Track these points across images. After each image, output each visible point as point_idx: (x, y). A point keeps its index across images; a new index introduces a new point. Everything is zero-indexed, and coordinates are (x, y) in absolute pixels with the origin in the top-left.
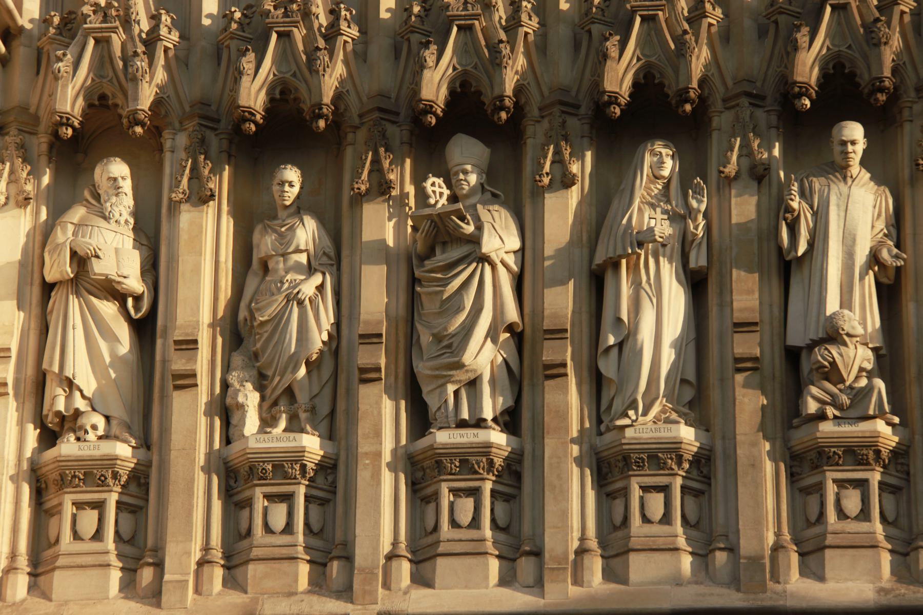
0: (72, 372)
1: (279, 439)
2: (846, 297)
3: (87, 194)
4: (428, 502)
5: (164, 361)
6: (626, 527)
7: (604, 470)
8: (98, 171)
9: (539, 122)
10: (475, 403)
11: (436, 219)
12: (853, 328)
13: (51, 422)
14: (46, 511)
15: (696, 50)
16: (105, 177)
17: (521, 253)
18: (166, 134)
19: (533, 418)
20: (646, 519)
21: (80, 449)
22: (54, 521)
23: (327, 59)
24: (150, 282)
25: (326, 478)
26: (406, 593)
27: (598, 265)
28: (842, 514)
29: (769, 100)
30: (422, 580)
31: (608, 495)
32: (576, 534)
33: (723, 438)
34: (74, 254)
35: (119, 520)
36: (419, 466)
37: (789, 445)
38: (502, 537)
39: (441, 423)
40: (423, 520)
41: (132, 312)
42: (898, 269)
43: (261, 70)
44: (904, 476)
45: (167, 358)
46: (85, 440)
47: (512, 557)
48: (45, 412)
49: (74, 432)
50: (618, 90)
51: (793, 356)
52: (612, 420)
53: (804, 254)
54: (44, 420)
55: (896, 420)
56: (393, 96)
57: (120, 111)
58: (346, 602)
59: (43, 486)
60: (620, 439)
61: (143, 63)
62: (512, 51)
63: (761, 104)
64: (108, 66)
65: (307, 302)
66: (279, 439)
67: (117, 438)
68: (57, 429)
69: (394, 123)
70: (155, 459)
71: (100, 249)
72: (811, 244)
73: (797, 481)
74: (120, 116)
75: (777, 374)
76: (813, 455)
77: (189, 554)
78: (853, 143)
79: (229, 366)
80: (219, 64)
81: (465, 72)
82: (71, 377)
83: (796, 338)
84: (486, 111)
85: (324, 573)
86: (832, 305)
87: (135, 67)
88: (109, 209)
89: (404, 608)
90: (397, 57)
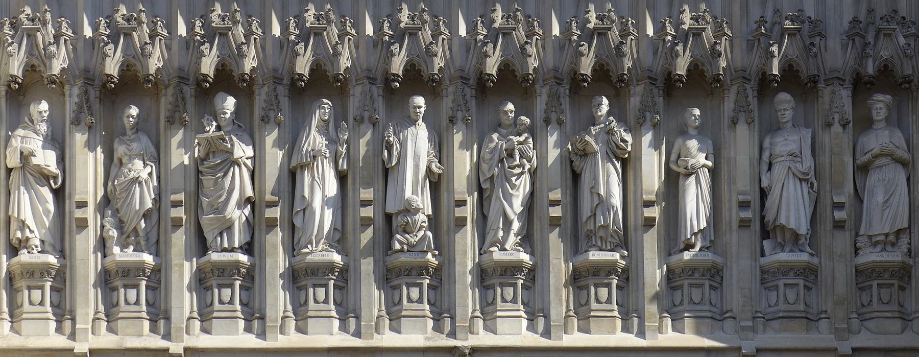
0: (24, 217)
1: (131, 256)
2: (414, 188)
3: (26, 119)
4: (208, 290)
5: (71, 212)
6: (306, 305)
7: (296, 275)
8: (32, 107)
9: (262, 87)
10: (231, 239)
11: (210, 140)
12: (418, 205)
13: (15, 242)
14: (15, 289)
15: (343, 52)
16: (36, 111)
17: (253, 158)
18: (67, 87)
19: (260, 247)
20: (316, 301)
21: (30, 258)
22: (19, 294)
23: (151, 49)
24: (61, 168)
25: (156, 277)
26: (197, 337)
27: (293, 167)
28: (410, 300)
29: (378, 81)
30: (206, 330)
31: (297, 288)
32: (282, 309)
33: (354, 260)
34: (22, 153)
35: (52, 296)
36: (203, 271)
37: (386, 264)
38: (245, 309)
39: (213, 249)
40: (205, 299)
41: (53, 184)
42: (440, 175)
43: (116, 54)
44: (440, 281)
45: (72, 211)
46: (32, 253)
47: (250, 319)
48: (11, 238)
49: (27, 248)
50: (303, 73)
51: (389, 218)
52: (300, 249)
53: (396, 164)
54: (11, 242)
55: (437, 253)
56: (186, 70)
57: (43, 75)
58: (168, 341)
59: (13, 276)
60: (304, 260)
61: (54, 49)
62: (248, 48)
63: (374, 83)
64: (35, 48)
65: (144, 182)
66: (131, 256)
67: (48, 252)
68: (17, 246)
69: (187, 84)
70: (68, 264)
71: (35, 151)
72: (398, 160)
73: (390, 282)
74: (43, 77)
75: (381, 227)
76: (397, 270)
77: (88, 314)
78: (420, 107)
79: (104, 216)
80: (93, 49)
81: (223, 59)
82: (24, 220)
83: (390, 209)
84: (235, 81)
85: (156, 325)
86: (408, 193)
87: (50, 50)
88: (39, 128)
89: (197, 345)
90: (188, 48)
